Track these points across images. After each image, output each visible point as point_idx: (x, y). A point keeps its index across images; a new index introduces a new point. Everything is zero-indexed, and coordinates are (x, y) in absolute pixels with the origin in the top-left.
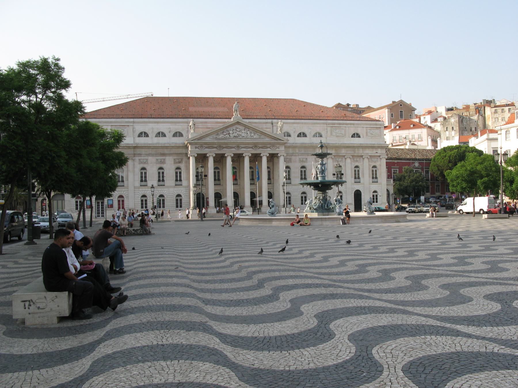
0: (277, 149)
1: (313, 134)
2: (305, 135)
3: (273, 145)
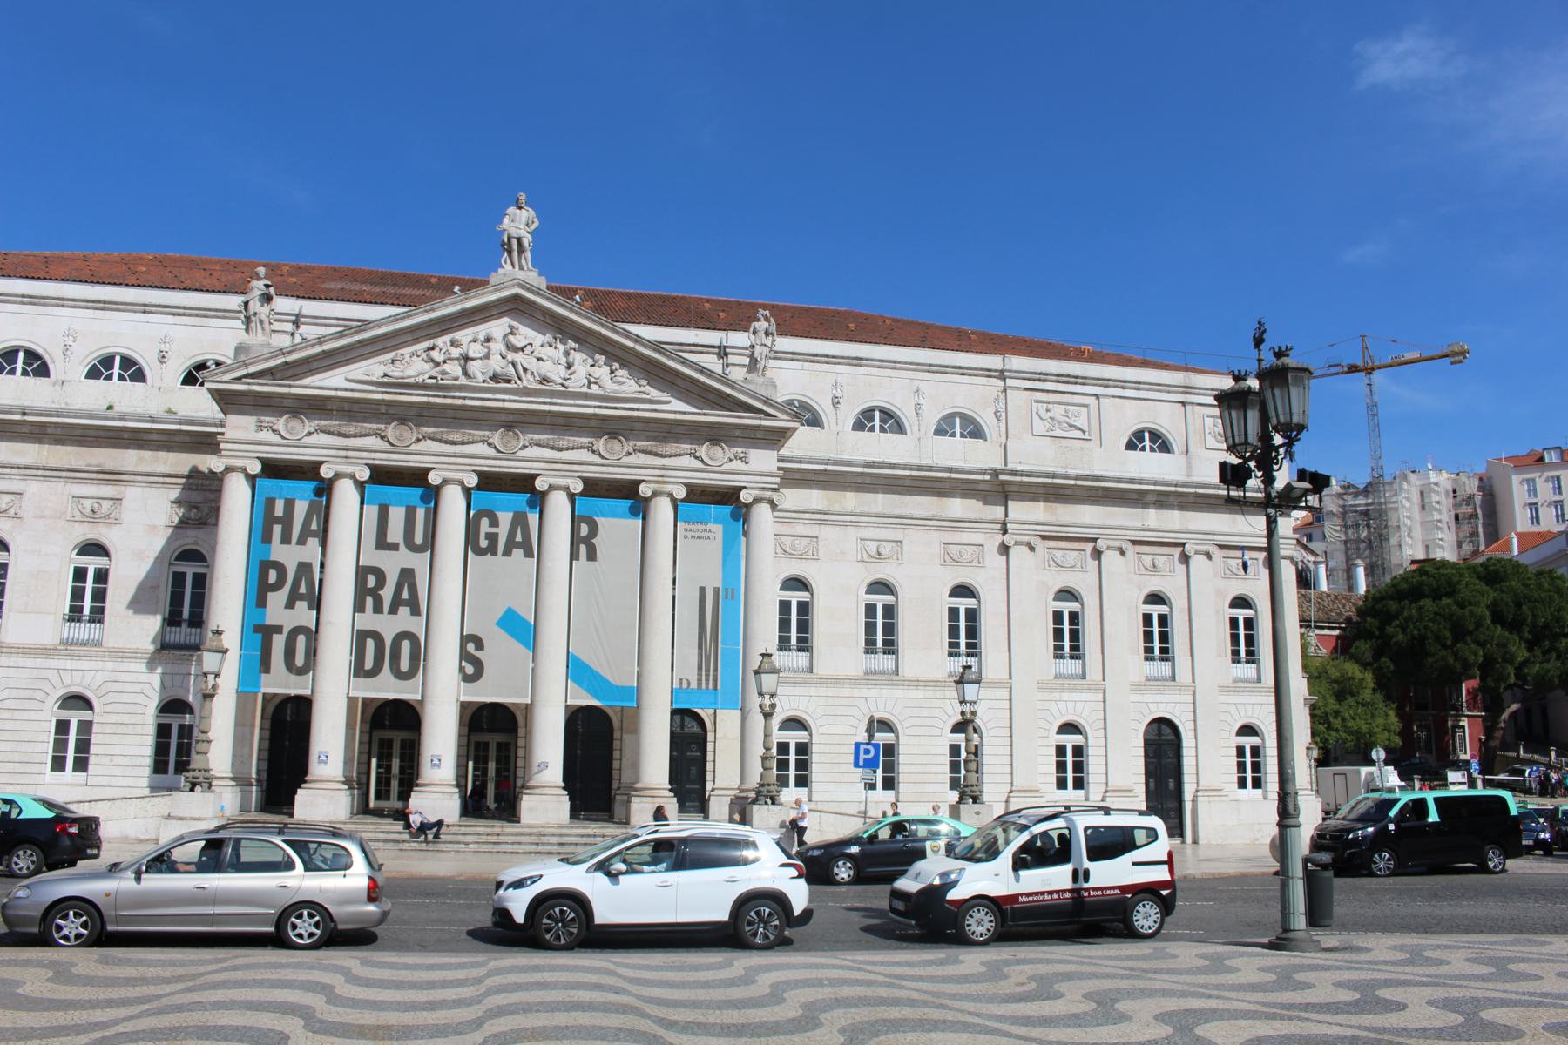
0: (737, 465)
1: (932, 418)
2: (891, 421)
3: (715, 435)
